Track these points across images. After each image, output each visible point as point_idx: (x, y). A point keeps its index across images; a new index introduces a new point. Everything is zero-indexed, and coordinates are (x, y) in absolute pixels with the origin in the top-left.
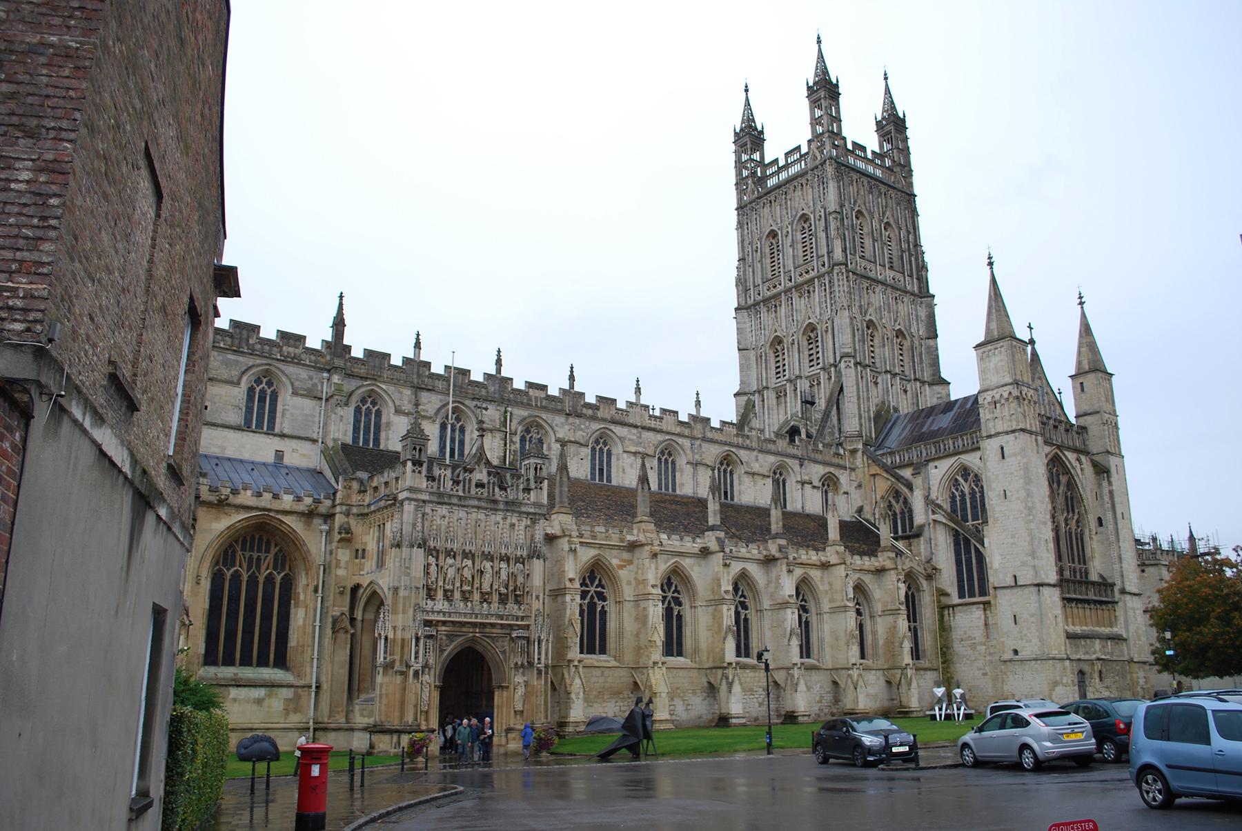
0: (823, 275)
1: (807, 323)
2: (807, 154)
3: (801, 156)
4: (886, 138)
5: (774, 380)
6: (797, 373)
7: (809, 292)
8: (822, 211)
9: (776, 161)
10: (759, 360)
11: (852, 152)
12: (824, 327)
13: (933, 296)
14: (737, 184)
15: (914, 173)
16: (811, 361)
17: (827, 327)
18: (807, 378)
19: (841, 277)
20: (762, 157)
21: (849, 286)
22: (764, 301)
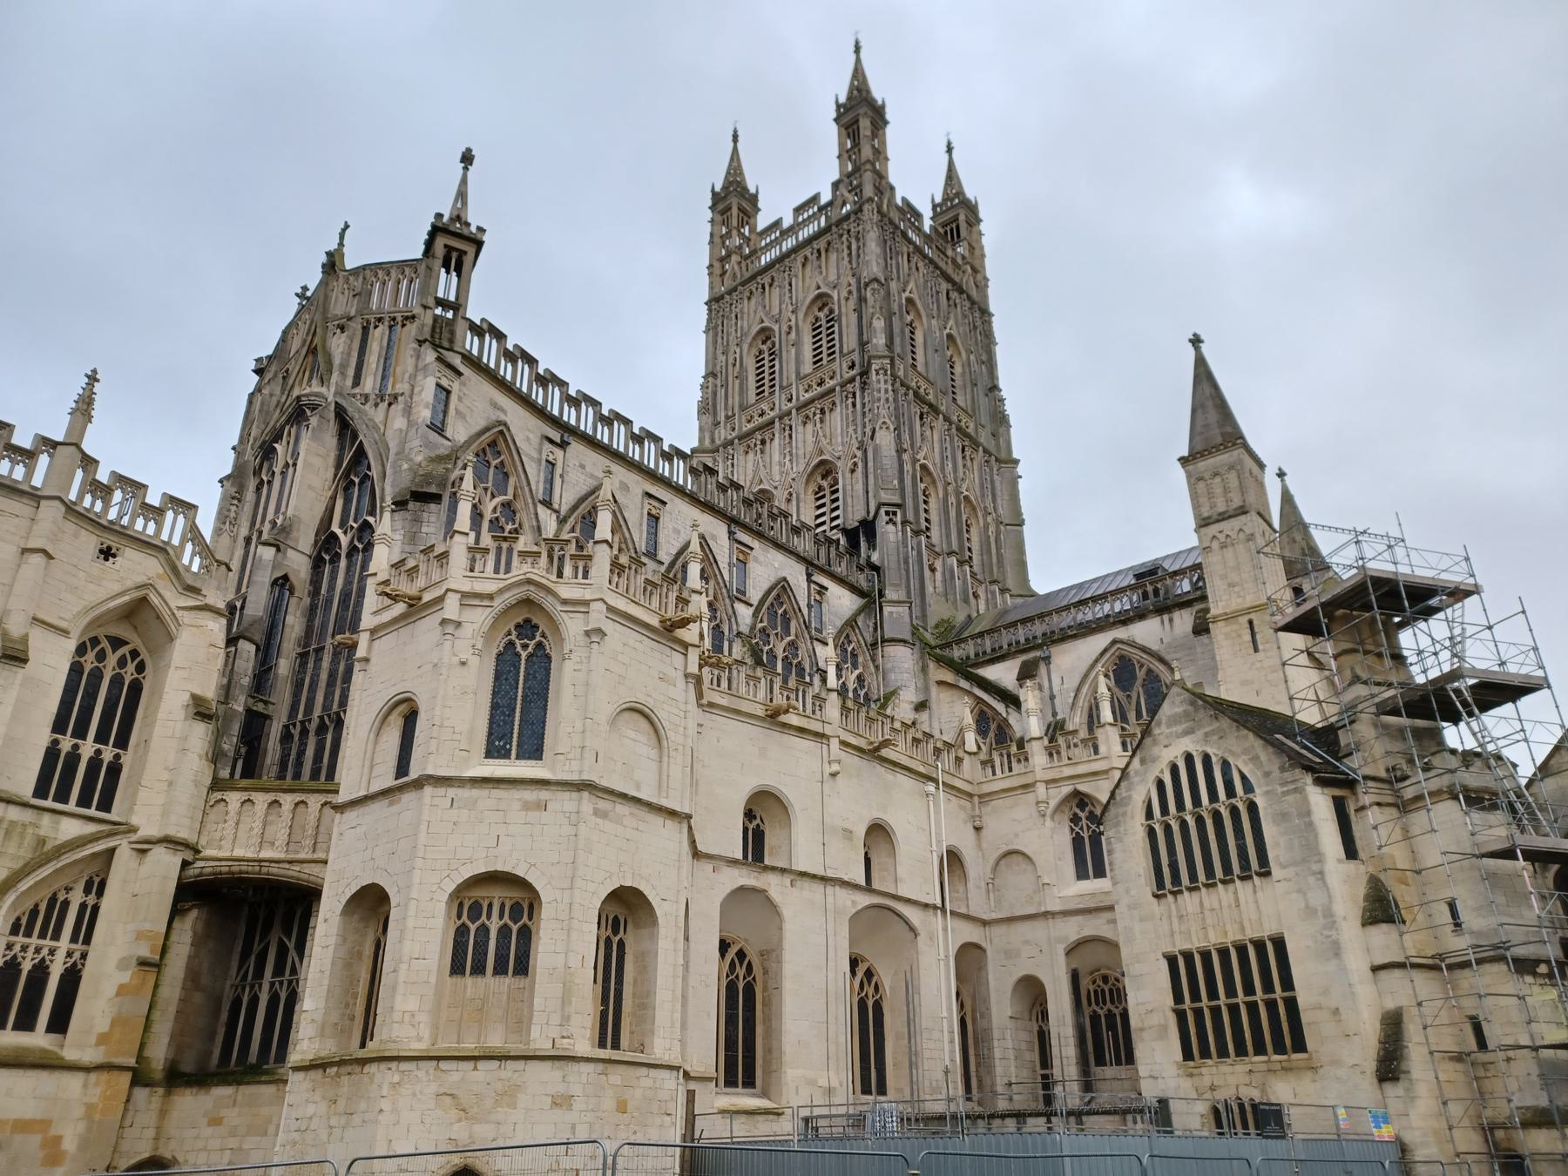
0: (852, 380)
1: (815, 461)
2: (830, 204)
3: (821, 209)
8: (853, 281)
12: (850, 464)
13: (1016, 462)
14: (710, 266)
15: (990, 284)
20: (752, 230)
21: (895, 400)
22: (740, 438)
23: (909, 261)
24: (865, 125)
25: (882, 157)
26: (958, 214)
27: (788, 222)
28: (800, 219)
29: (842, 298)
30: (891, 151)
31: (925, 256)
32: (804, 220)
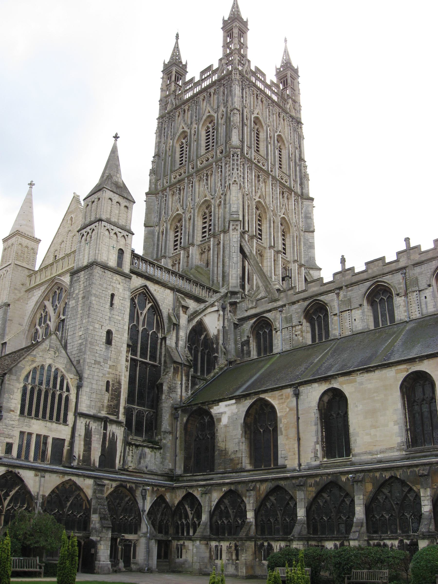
0: (221, 159)
2: (217, 69)
4: (282, 81)
5: (172, 251)
6: (191, 242)
7: (207, 175)
9: (192, 80)
10: (161, 235)
11: (254, 74)
12: (218, 202)
13: (312, 199)
14: (161, 101)
15: (302, 108)
16: (204, 233)
17: (220, 202)
18: (199, 246)
19: (235, 158)
23: (257, 99)
24: (236, 31)
25: (244, 47)
26: (287, 73)
27: (197, 79)
28: (203, 77)
29: (219, 117)
30: (250, 43)
31: (267, 96)
32: (205, 78)
